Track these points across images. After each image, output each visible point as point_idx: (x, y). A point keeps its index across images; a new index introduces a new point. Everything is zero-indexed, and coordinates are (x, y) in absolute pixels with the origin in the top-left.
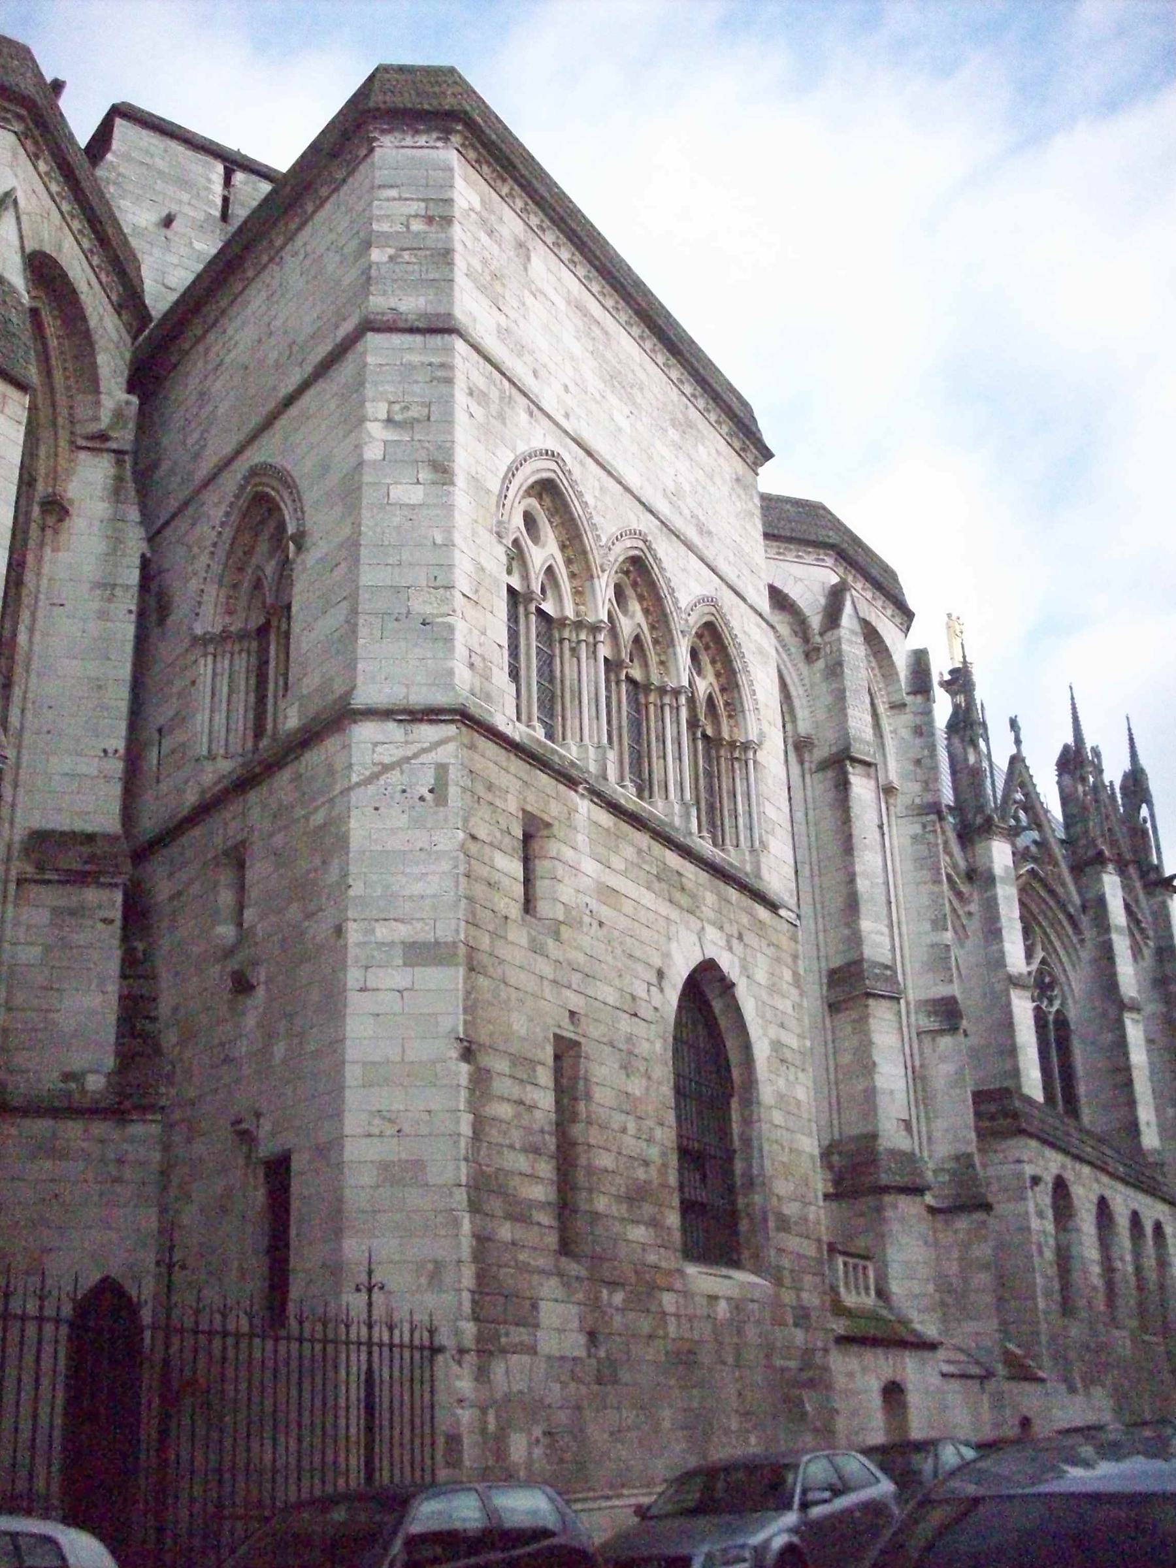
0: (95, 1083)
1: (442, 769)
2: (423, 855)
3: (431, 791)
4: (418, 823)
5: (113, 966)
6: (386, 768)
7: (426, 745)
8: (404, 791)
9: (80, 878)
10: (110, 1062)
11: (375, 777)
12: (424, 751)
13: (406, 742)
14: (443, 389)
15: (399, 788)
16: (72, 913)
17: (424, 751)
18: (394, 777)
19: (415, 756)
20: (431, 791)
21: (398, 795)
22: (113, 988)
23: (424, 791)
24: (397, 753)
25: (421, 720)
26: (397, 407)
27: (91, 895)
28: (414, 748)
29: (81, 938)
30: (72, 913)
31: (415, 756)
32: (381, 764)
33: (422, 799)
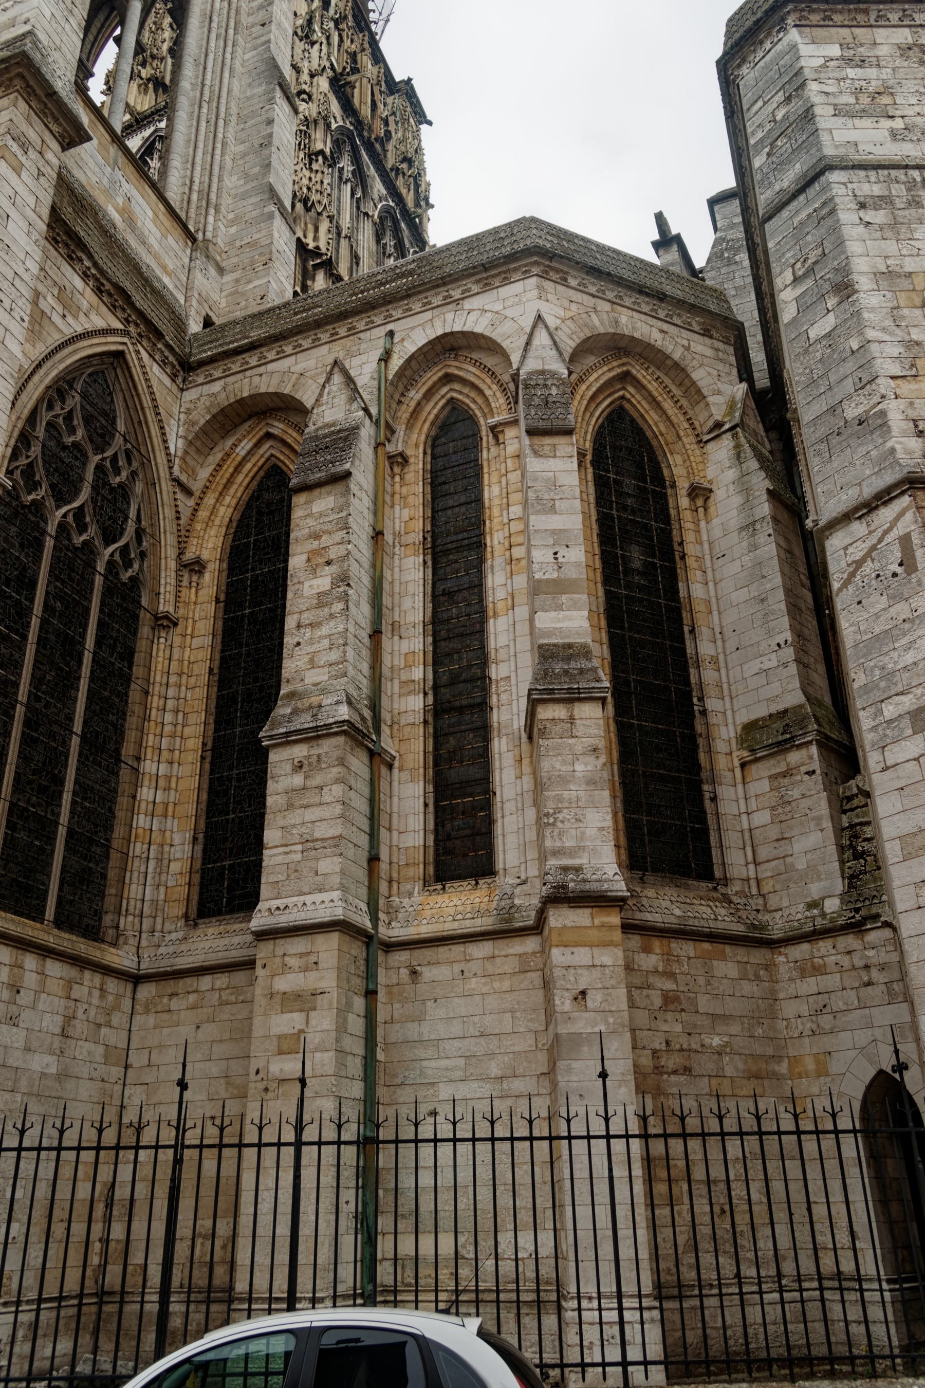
0: (832, 905)
1: (905, 540)
2: (907, 626)
3: (901, 565)
4: (897, 598)
5: (823, 808)
6: (859, 564)
7: (885, 527)
8: (878, 576)
9: (783, 746)
10: (839, 886)
11: (852, 574)
12: (886, 532)
13: (870, 533)
14: (829, 222)
15: (873, 575)
16: (784, 775)
17: (886, 532)
18: (869, 568)
19: (880, 540)
20: (901, 565)
21: (874, 582)
22: (827, 824)
23: (895, 568)
24: (865, 546)
25: (877, 507)
26: (799, 265)
27: (794, 757)
28: (879, 533)
29: (795, 793)
30: (784, 775)
31: (880, 540)
32: (854, 562)
33: (895, 575)
